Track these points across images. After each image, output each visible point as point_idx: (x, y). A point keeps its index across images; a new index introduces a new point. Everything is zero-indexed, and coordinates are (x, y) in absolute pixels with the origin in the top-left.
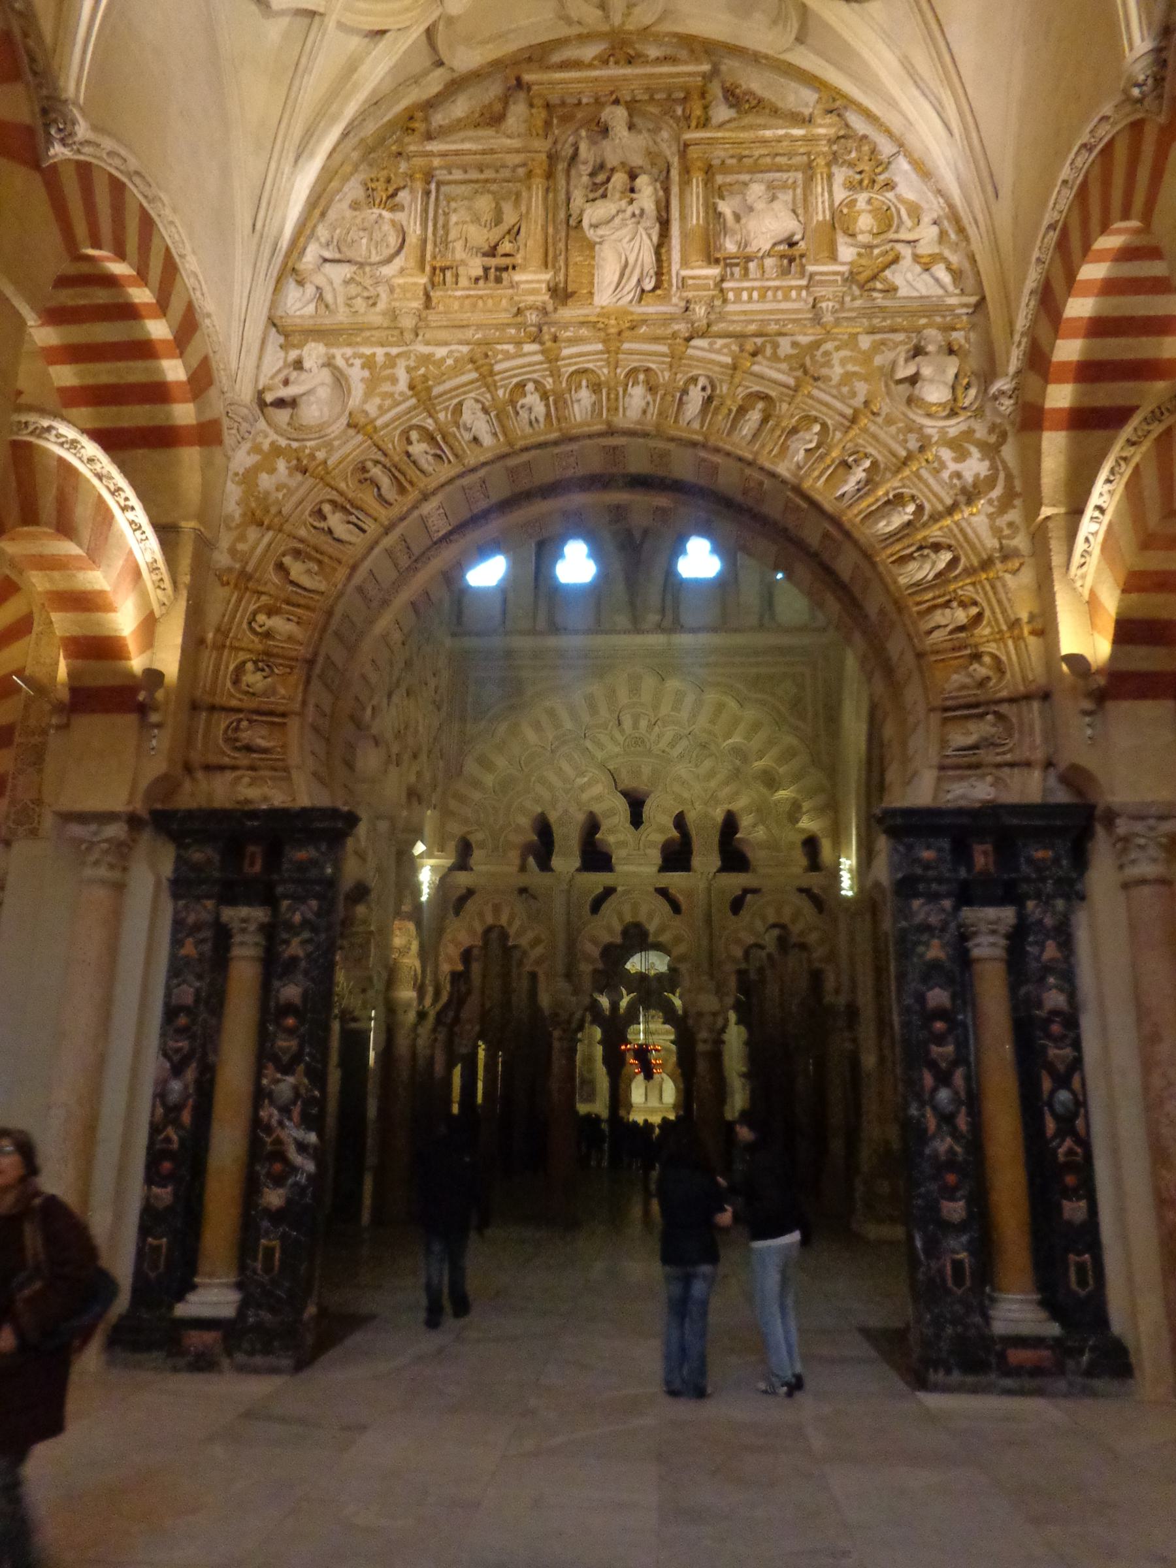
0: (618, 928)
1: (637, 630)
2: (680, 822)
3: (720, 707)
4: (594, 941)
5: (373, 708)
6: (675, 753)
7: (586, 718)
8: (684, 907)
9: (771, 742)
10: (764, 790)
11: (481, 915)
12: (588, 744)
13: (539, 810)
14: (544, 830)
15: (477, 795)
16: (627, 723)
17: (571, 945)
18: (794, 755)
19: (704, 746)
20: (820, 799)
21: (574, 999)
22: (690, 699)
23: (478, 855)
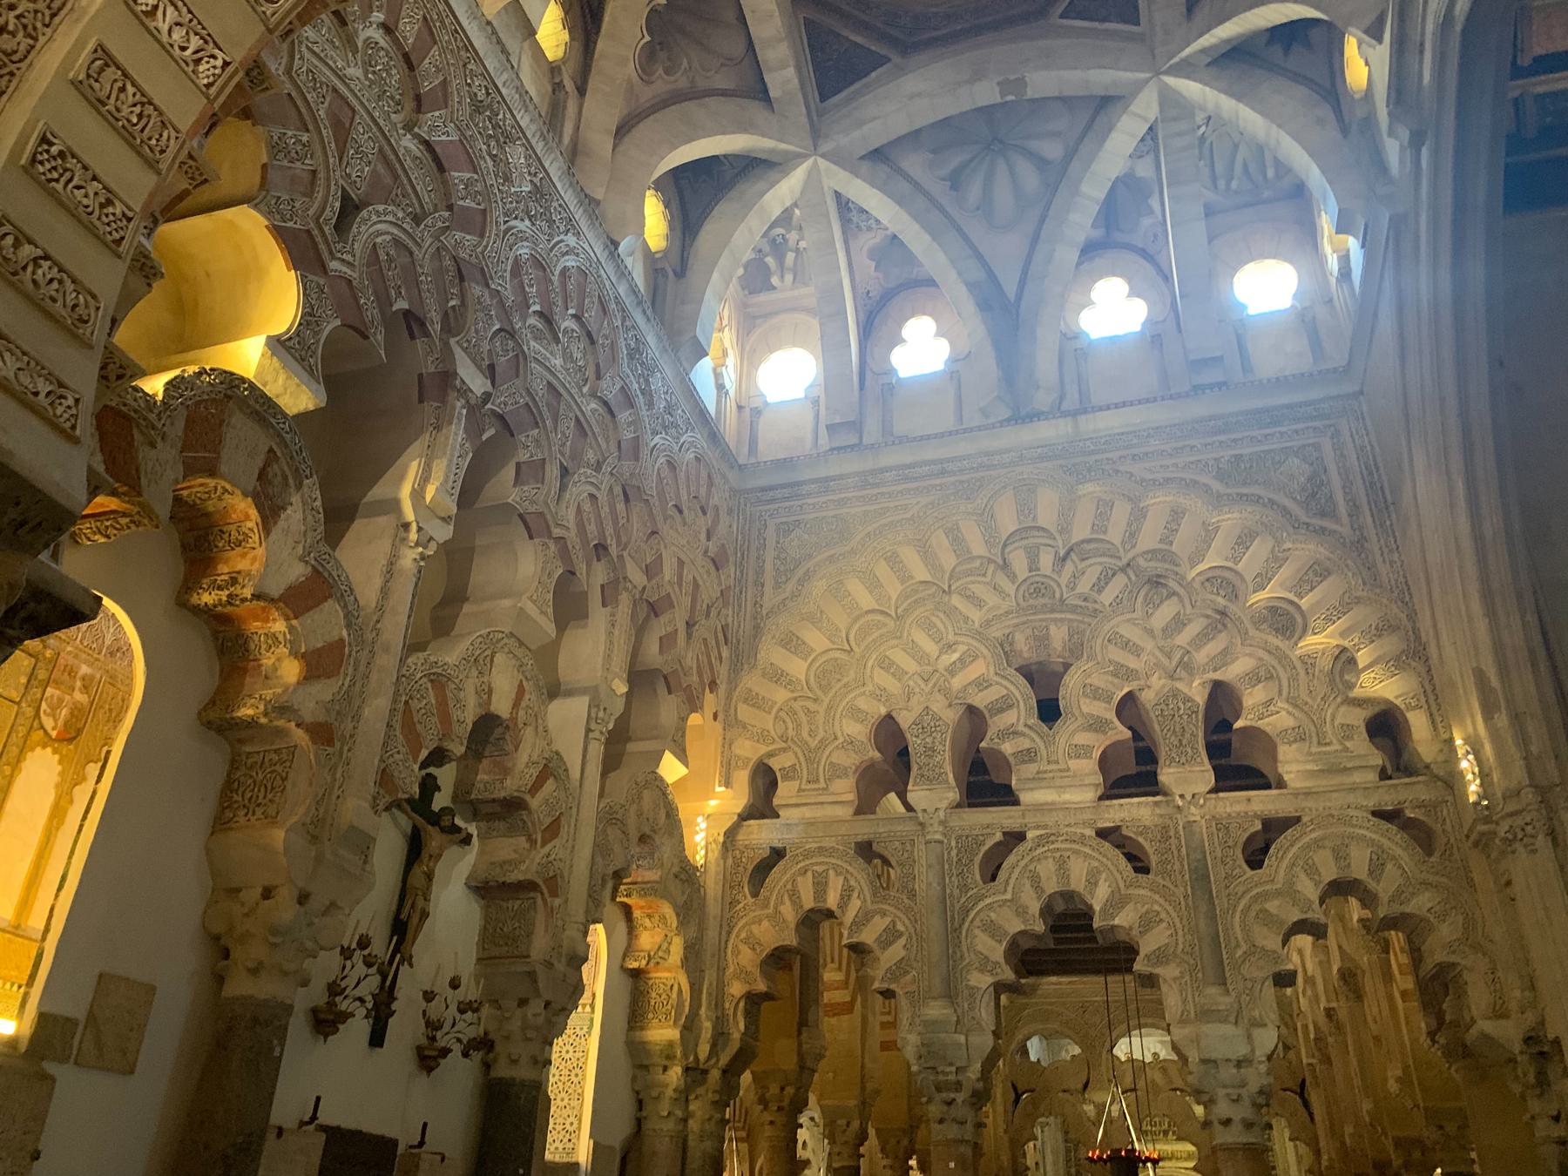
0: (1035, 907)
1: (1022, 416)
2: (1128, 707)
3: (1177, 515)
4: (992, 929)
5: (518, 465)
6: (1107, 597)
7: (949, 560)
8: (1154, 860)
9: (1278, 559)
10: (1275, 641)
11: (794, 895)
12: (956, 600)
13: (883, 711)
14: (890, 735)
15: (780, 695)
16: (1019, 562)
17: (953, 935)
18: (1324, 574)
19: (1156, 582)
20: (1391, 644)
21: (962, 1038)
22: (1121, 514)
23: (785, 792)
